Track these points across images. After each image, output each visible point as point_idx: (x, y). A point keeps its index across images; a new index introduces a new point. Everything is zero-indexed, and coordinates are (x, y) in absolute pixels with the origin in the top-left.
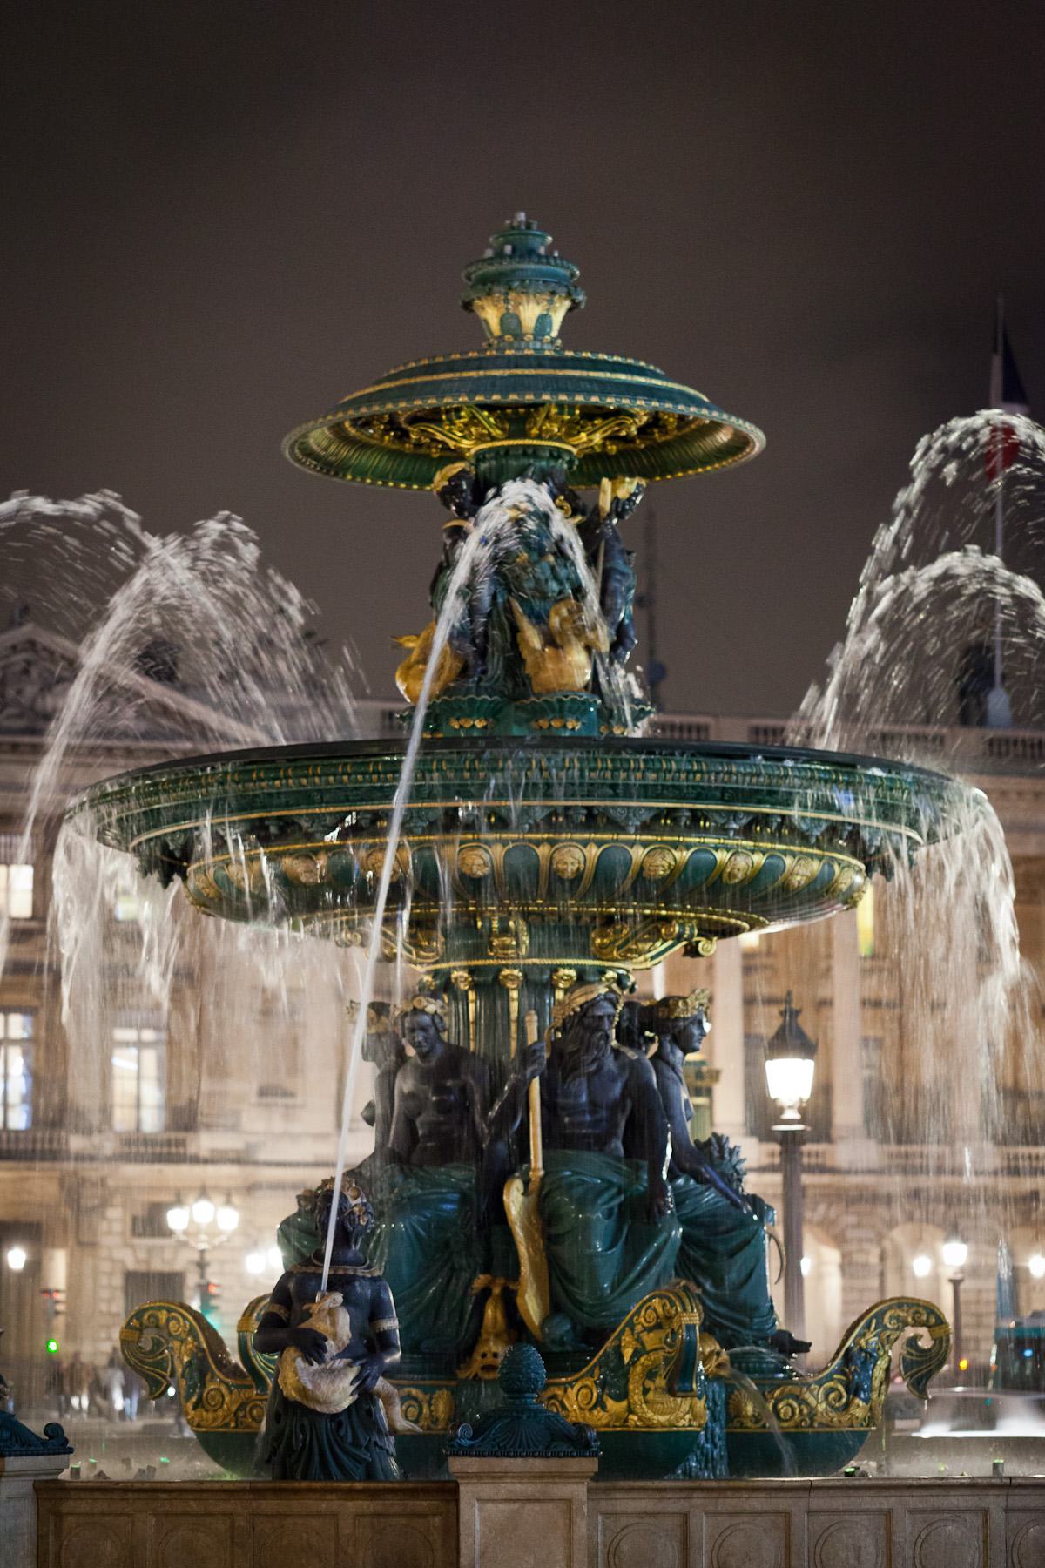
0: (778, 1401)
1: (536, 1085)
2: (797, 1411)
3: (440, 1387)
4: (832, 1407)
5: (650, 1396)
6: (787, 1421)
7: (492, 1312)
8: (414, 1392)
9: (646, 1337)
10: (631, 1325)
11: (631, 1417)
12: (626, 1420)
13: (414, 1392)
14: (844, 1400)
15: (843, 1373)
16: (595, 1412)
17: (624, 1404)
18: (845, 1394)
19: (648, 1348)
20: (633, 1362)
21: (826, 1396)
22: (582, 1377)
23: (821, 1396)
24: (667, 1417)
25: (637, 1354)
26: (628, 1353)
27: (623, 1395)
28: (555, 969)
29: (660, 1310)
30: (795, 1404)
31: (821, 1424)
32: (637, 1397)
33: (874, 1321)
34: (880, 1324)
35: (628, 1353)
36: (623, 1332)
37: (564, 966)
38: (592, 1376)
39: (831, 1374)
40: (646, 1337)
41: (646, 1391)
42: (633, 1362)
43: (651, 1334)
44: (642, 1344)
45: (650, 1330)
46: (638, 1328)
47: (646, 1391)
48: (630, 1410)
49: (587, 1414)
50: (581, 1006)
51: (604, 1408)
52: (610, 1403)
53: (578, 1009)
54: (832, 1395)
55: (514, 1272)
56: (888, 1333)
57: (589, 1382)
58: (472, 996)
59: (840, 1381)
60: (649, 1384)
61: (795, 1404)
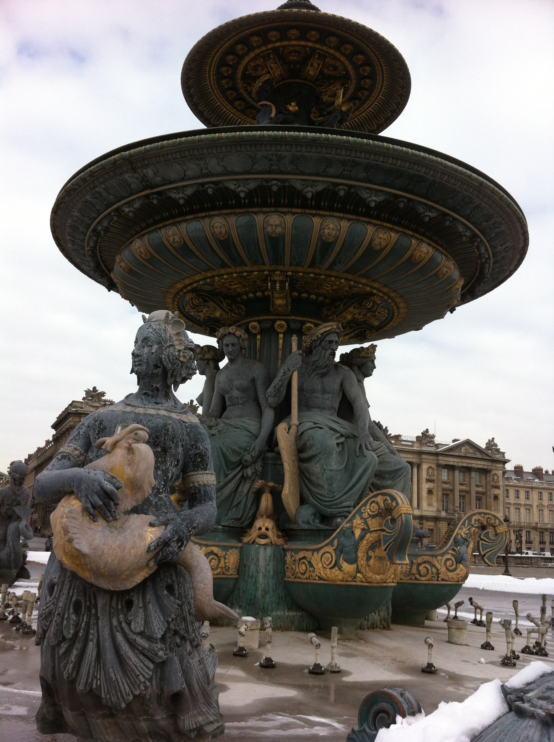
0: (420, 564)
1: (295, 374)
2: (430, 571)
3: (232, 547)
4: (448, 570)
5: (372, 562)
6: (424, 576)
7: (266, 501)
8: (215, 550)
9: (370, 521)
10: (359, 512)
11: (359, 575)
12: (355, 577)
13: (215, 550)
14: (454, 566)
15: (454, 550)
16: (334, 570)
17: (354, 566)
18: (455, 563)
19: (371, 530)
20: (362, 538)
21: (445, 564)
22: (326, 545)
23: (443, 564)
24: (381, 576)
25: (365, 531)
26: (358, 533)
27: (353, 560)
28: (303, 323)
29: (382, 505)
30: (429, 567)
31: (443, 580)
32: (362, 562)
33: (467, 521)
34: (470, 524)
35: (358, 533)
36: (354, 516)
37: (309, 322)
38: (332, 546)
39: (447, 550)
40: (370, 521)
41: (369, 558)
42: (362, 538)
43: (374, 520)
44: (368, 526)
45: (373, 517)
46: (365, 515)
47: (369, 558)
48: (358, 571)
49: (328, 571)
50: (322, 334)
51: (340, 569)
52: (345, 566)
53: (320, 336)
54: (448, 563)
55: (281, 481)
56: (474, 529)
57: (330, 549)
58: (259, 337)
59: (452, 554)
60: (371, 553)
61: (429, 567)
